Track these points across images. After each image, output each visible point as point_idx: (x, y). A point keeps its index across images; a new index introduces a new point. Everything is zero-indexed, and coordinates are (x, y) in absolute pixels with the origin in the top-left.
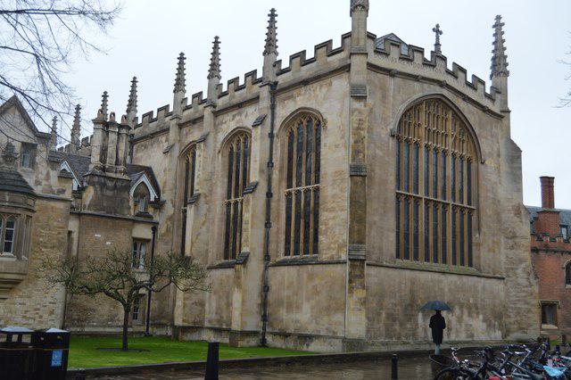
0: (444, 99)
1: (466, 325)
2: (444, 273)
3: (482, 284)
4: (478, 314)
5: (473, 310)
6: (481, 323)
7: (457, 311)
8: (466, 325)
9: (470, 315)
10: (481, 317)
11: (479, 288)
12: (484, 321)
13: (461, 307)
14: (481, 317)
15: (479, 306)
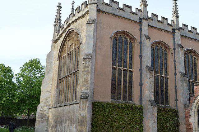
0: (70, 30)
1: (70, 129)
2: (65, 106)
3: (76, 108)
4: (74, 124)
5: (72, 122)
6: (74, 128)
7: (67, 123)
8: (70, 129)
9: (71, 125)
10: (75, 125)
11: (75, 111)
12: (76, 127)
13: (69, 121)
14: (75, 125)
15: (75, 119)
